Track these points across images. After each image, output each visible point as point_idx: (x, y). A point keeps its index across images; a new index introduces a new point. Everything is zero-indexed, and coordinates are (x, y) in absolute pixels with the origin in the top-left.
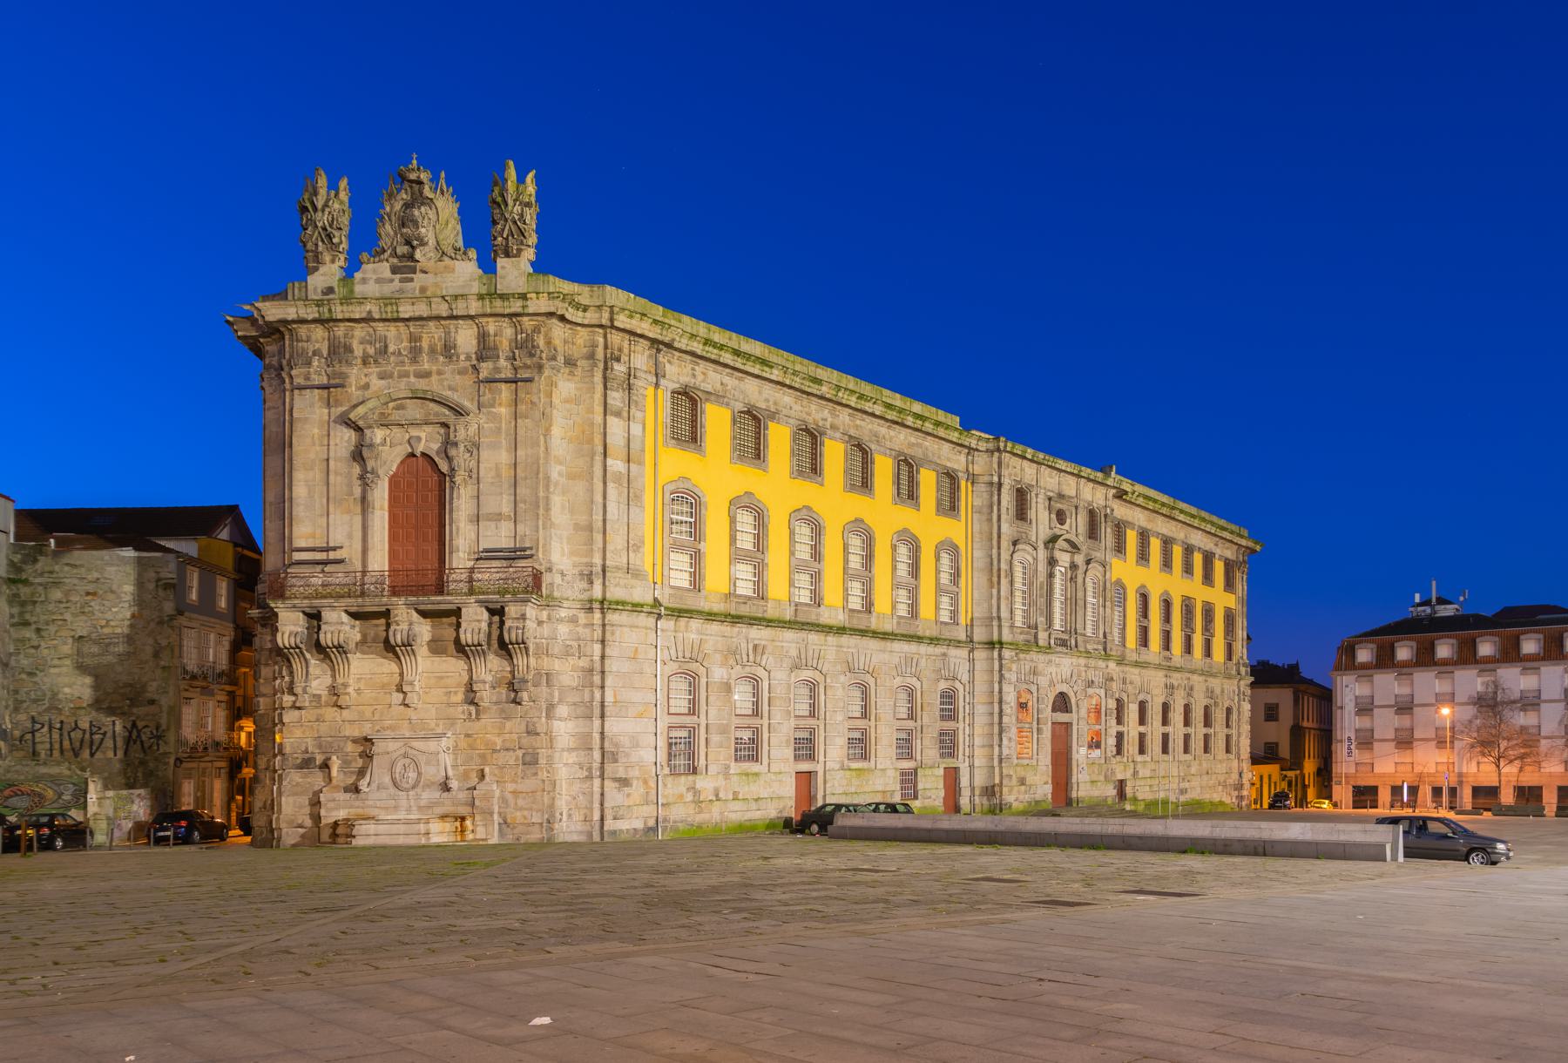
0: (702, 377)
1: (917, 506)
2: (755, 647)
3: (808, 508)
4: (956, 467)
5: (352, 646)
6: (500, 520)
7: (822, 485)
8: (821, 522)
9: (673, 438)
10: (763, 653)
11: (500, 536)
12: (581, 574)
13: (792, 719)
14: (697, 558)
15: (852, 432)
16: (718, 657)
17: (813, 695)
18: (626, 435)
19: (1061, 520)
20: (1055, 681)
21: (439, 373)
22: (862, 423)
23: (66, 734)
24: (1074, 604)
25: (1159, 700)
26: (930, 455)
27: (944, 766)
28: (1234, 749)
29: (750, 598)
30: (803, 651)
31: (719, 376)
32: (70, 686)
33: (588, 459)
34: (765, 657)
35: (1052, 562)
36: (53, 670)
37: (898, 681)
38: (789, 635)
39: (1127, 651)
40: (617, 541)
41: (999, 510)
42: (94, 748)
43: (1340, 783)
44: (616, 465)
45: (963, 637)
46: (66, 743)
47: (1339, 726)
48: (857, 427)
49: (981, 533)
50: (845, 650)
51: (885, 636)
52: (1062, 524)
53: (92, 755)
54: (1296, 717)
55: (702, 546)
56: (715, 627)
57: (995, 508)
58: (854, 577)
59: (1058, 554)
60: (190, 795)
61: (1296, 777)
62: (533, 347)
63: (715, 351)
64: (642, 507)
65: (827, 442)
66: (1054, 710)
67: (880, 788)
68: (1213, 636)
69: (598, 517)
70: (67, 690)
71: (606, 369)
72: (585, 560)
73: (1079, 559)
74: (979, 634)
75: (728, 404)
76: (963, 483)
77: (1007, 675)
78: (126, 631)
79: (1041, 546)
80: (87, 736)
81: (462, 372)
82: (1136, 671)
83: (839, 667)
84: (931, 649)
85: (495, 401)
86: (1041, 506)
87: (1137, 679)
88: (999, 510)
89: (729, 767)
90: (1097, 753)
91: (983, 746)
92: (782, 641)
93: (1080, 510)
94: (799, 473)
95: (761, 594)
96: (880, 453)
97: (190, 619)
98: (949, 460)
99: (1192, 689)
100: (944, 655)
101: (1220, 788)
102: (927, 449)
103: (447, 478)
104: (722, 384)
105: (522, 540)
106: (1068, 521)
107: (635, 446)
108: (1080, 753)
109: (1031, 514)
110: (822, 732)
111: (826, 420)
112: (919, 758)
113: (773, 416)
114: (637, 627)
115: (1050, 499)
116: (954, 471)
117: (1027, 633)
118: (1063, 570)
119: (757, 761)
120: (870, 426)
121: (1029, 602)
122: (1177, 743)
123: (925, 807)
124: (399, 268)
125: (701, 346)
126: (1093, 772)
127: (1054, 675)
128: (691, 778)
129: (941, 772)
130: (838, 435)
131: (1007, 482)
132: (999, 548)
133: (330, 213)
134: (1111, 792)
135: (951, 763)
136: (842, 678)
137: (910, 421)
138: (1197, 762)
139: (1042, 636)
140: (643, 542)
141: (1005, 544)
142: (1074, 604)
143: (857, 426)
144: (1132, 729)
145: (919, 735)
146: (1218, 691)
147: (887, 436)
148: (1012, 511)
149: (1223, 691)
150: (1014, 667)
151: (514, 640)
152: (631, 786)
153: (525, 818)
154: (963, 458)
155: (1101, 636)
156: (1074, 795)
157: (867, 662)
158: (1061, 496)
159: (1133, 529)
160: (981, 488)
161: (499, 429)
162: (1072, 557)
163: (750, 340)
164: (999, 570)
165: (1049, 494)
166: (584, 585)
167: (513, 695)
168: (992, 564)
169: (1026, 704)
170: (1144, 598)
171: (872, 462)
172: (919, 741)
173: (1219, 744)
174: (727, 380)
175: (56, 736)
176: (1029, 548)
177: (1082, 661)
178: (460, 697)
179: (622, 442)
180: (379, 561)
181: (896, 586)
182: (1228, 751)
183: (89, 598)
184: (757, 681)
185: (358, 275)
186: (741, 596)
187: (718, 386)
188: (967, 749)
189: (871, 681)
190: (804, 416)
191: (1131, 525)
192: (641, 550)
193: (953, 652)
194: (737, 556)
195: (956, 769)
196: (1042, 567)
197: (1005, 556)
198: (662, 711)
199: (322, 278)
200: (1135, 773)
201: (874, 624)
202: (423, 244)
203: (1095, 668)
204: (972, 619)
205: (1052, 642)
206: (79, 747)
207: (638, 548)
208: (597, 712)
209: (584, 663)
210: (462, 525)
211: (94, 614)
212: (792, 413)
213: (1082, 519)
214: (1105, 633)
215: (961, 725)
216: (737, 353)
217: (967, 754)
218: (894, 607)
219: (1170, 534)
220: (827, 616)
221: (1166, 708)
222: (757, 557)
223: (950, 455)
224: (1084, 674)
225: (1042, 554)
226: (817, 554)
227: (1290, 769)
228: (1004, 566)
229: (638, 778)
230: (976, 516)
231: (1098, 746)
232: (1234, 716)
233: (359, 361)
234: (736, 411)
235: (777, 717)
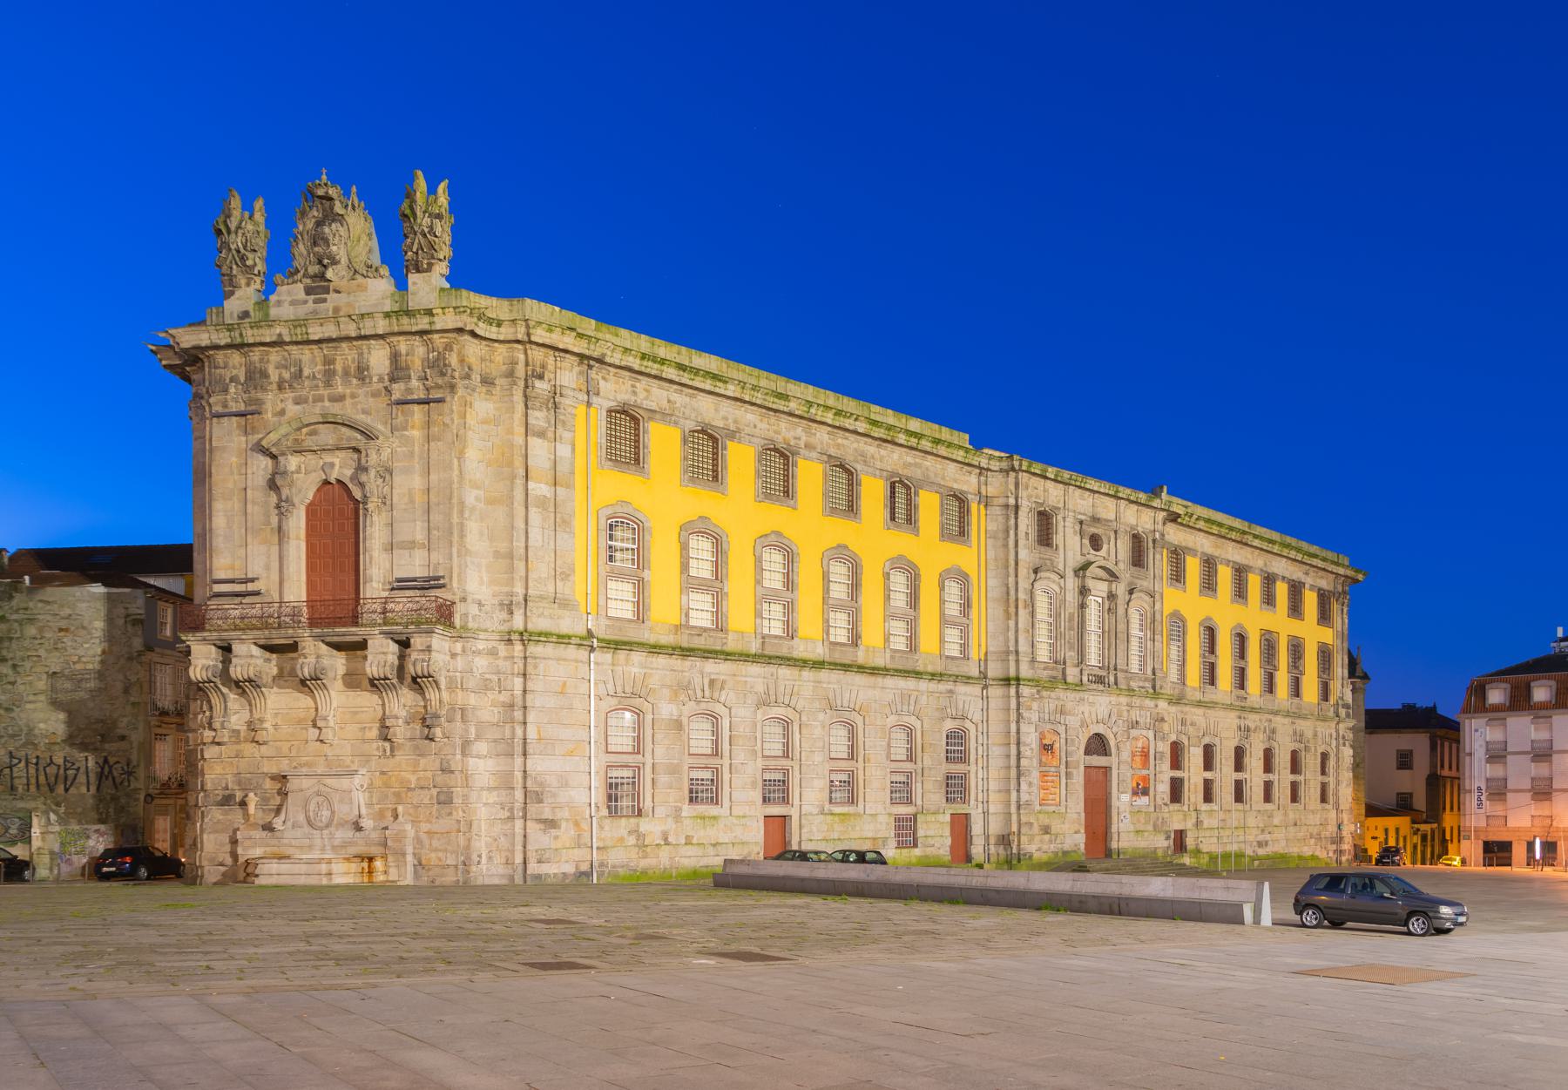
0: (645, 394)
1: (916, 532)
2: (712, 682)
3: (778, 534)
4: (965, 488)
5: (267, 679)
6: (414, 548)
7: (795, 508)
8: (794, 548)
9: (611, 460)
10: (722, 688)
11: (414, 565)
12: (501, 604)
13: (759, 760)
14: (641, 587)
15: (832, 452)
16: (666, 692)
17: (787, 734)
18: (553, 457)
19: (1096, 542)
20: (1088, 721)
21: (353, 396)
22: (845, 442)
23: (41, 769)
24: (1113, 636)
25: (1234, 743)
26: (932, 475)
27: (951, 811)
28: (1331, 799)
29: (705, 630)
30: (772, 687)
31: (665, 393)
32: (45, 722)
33: (508, 483)
34: (723, 692)
35: (1084, 591)
36: (28, 706)
37: (892, 720)
38: (755, 669)
39: (1188, 690)
40: (541, 569)
41: (1016, 535)
42: (69, 783)
43: (1469, 838)
44: (539, 488)
45: (975, 672)
46: (42, 779)
47: (1467, 774)
49: (996, 560)
50: (825, 686)
51: (874, 671)
52: (1097, 550)
53: (66, 790)
54: (1433, 765)
55: (646, 574)
57: (1012, 533)
58: (839, 607)
59: (1090, 583)
60: (165, 831)
61: (1433, 831)
62: (445, 365)
63: (656, 366)
64: (572, 533)
65: (801, 462)
66: (1088, 752)
67: (870, 835)
68: (1302, 673)
69: (519, 544)
70: (42, 726)
71: (526, 387)
72: (506, 589)
73: (1121, 589)
74: (994, 670)
76: (974, 507)
77: (1025, 714)
78: (97, 666)
79: (1070, 574)
80: (62, 771)
81: (375, 395)
82: (1200, 711)
83: (817, 705)
84: (933, 686)
85: (407, 425)
86: (1069, 531)
87: (1201, 721)
88: (1016, 535)
89: (681, 809)
90: (1145, 800)
91: (1000, 791)
92: (746, 676)
93: (1120, 535)
94: (766, 495)
95: (720, 627)
96: (867, 474)
97: (163, 655)
98: (955, 481)
99: (1273, 731)
100: (951, 692)
101: (1313, 841)
102: (927, 469)
103: (361, 505)
104: (669, 401)
105: (436, 569)
106: (1105, 547)
107: (563, 468)
108: (1122, 800)
109: (1058, 539)
110: (797, 773)
111: (799, 439)
112: (919, 802)
113: (733, 435)
114: (565, 660)
115: (1081, 523)
116: (962, 492)
117: (1053, 669)
118: (1100, 600)
119: (717, 803)
120: (855, 445)
121: (1056, 635)
122: (1255, 789)
123: (926, 856)
124: (312, 287)
125: (638, 361)
126: (1139, 821)
127: (1086, 715)
128: (633, 820)
129: (948, 818)
130: (814, 455)
131: (1025, 505)
132: (1016, 576)
133: (243, 234)
134: (1162, 843)
135: (960, 809)
136: (821, 716)
137: (902, 438)
138: (1281, 811)
139: (1072, 673)
140: (574, 571)
141: (1023, 571)
142: (1113, 636)
143: (839, 445)
144: (1194, 773)
145: (919, 778)
146: (1309, 734)
147: (877, 456)
148: (1033, 535)
149: (1315, 735)
150: (1035, 705)
151: (420, 674)
152: (560, 828)
153: (440, 860)
154: (973, 479)
155: (1149, 672)
156: (1114, 845)
157: (853, 699)
158: (1095, 520)
159: (1195, 555)
160: (997, 511)
161: (412, 453)
162: (1110, 586)
163: (704, 354)
164: (1017, 600)
165: (1080, 517)
166: (504, 615)
167: (426, 730)
168: (1008, 593)
169: (1052, 746)
170: (1211, 633)
171: (859, 484)
172: (919, 785)
173: (1311, 793)
174: (675, 397)
175: (32, 771)
176: (1056, 577)
177: (1124, 700)
178: (374, 733)
179: (548, 465)
180: (297, 591)
181: (890, 616)
182: (1324, 799)
183: (62, 634)
184: (717, 719)
185: (273, 298)
186: (695, 627)
187: (665, 404)
188: (980, 795)
189: (859, 720)
190: (771, 434)
191: (1193, 552)
192: (570, 578)
193: (962, 689)
194: (690, 584)
195: (967, 816)
196: (1072, 597)
197: (1024, 584)
198: (597, 748)
199: (238, 302)
200: (1198, 824)
201: (861, 657)
202: (335, 262)
203: (1141, 708)
204: (986, 654)
205: (1085, 679)
206: (54, 783)
207: (567, 576)
208: (519, 749)
209: (504, 697)
210: (376, 554)
211: (66, 650)
212: (757, 431)
213: (1124, 548)
214: (1154, 669)
215: (973, 768)
216: (682, 367)
217: (980, 799)
218: (887, 640)
219: (1244, 562)
220: (800, 650)
221: (1239, 754)
222: (716, 586)
224: (1125, 714)
225: (1072, 583)
226: (790, 583)
227: (1426, 822)
228: (1022, 596)
229: (567, 820)
230: (990, 542)
231: (1145, 792)
232: (1332, 762)
233: (275, 386)
234: (687, 432)
235: (740, 756)
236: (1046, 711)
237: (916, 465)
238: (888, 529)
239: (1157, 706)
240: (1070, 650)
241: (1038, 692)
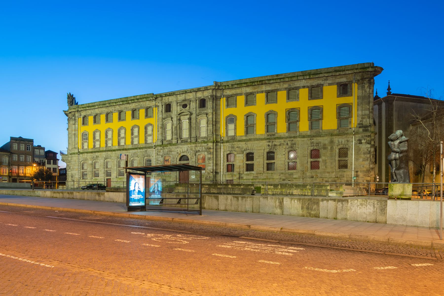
16: (90, 159)
22: (122, 107)
38: (104, 153)
48: (121, 108)
56: (89, 154)
75: (92, 115)
83: (115, 158)
84: (141, 150)
96: (127, 111)
100: (146, 151)
120: (124, 106)
127: (179, 151)
130: (116, 111)
147: (129, 107)
150: (161, 151)
169: (168, 160)
187: (90, 113)
223: (149, 103)
236: (165, 152)
237: (139, 105)
238: (132, 120)
239: (208, 145)
240: (175, 135)
241: (163, 148)
